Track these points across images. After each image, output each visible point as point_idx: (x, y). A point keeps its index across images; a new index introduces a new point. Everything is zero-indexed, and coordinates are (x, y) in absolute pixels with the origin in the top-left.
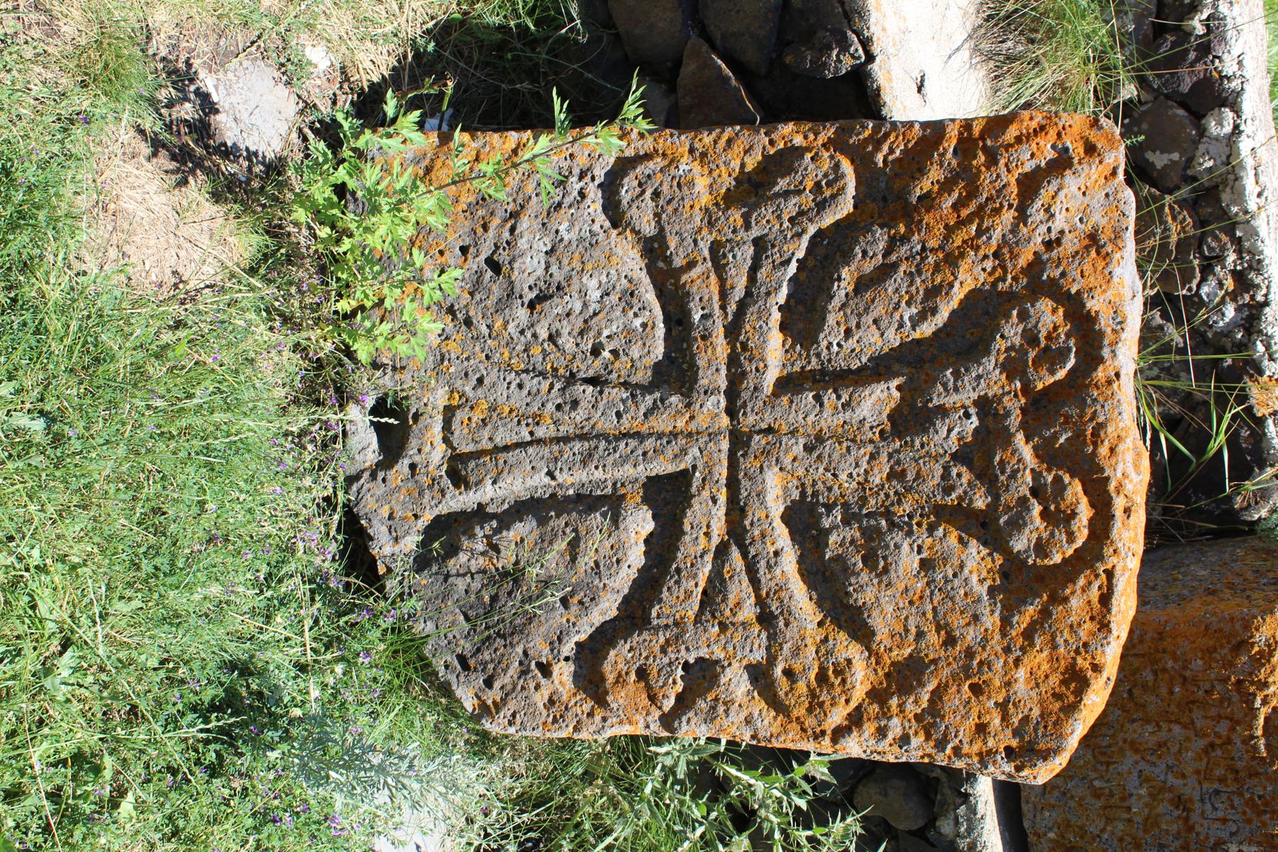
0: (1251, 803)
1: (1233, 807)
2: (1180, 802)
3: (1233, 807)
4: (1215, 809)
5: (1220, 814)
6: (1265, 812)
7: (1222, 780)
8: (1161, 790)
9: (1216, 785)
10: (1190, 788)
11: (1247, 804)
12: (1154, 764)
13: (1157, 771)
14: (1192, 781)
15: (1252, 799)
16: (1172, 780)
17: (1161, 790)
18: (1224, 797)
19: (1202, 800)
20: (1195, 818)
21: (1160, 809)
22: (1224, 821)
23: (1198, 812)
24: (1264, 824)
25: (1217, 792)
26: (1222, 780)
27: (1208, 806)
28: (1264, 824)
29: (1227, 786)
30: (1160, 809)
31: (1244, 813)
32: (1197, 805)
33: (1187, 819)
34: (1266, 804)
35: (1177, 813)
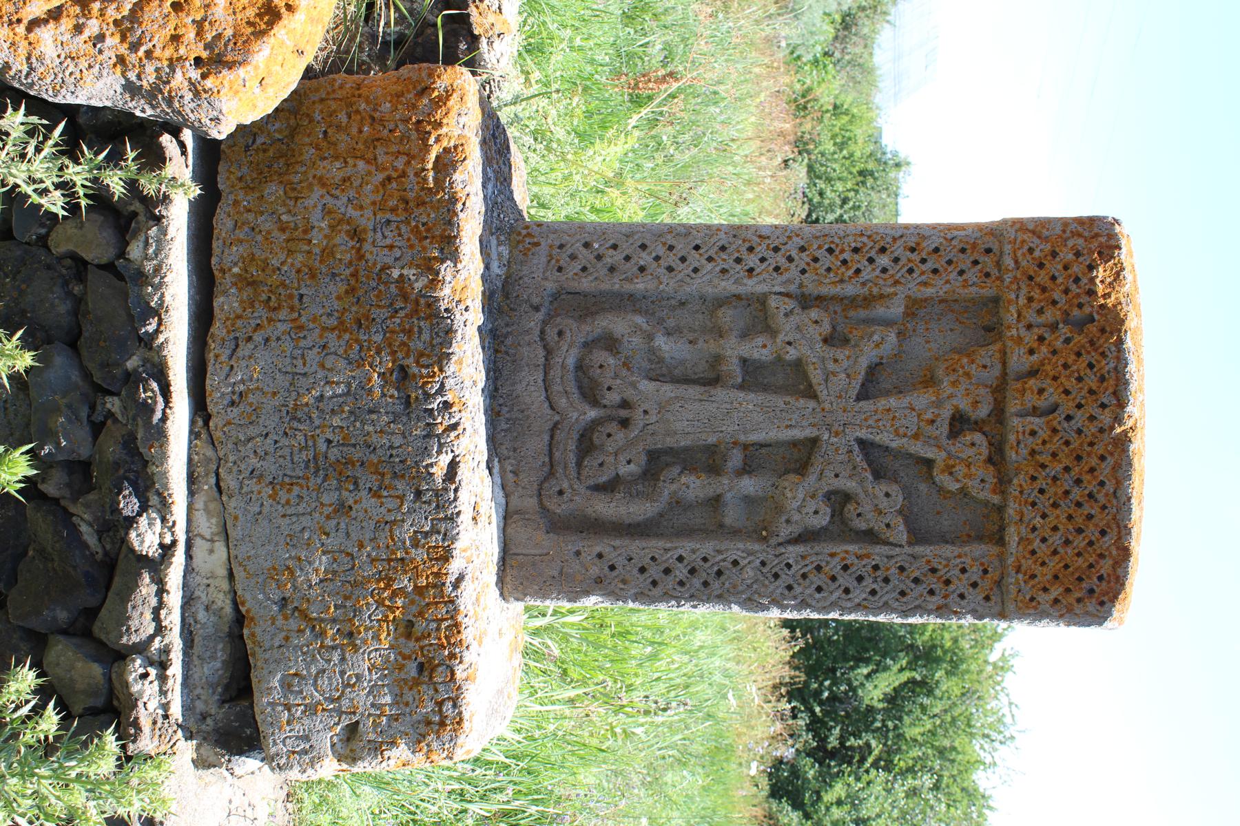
0: (416, 230)
1: (400, 235)
2: (356, 234)
3: (400, 235)
4: (385, 237)
5: (388, 242)
6: (426, 238)
7: (393, 210)
8: (340, 221)
9: (388, 216)
10: (366, 220)
11: (412, 231)
12: (337, 198)
13: (339, 203)
14: (368, 212)
15: (416, 227)
16: (352, 212)
17: (340, 221)
18: (394, 225)
19: (375, 230)
20: (367, 246)
21: (338, 240)
22: (391, 247)
23: (370, 240)
24: (424, 248)
25: (388, 222)
26: (393, 210)
27: (379, 235)
28: (424, 248)
29: (397, 215)
30: (338, 240)
31: (409, 239)
32: (370, 234)
33: (359, 250)
34: (428, 230)
35: (351, 243)
